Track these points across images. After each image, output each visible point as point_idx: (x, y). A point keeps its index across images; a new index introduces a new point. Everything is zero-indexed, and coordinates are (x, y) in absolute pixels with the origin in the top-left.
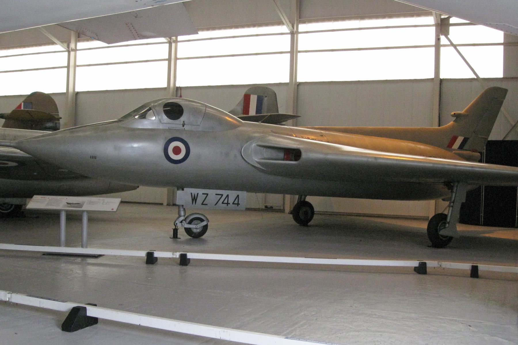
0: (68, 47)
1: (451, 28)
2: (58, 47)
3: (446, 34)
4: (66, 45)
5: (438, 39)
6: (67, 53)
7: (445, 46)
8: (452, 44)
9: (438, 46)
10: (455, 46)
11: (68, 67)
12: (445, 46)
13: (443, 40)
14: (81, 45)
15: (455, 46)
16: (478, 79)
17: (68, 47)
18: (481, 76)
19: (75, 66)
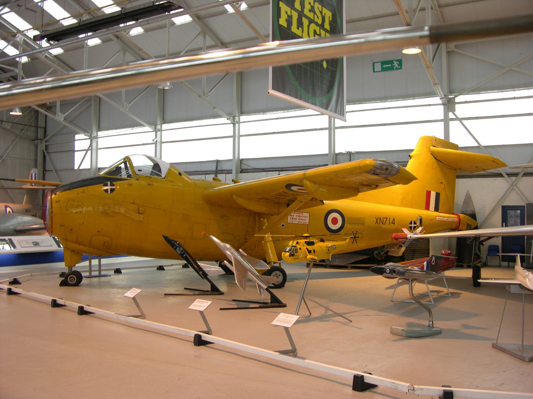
0: (155, 128)
1: (457, 106)
2: (147, 128)
3: (453, 111)
4: (153, 127)
6: (154, 133)
7: (452, 119)
8: (457, 119)
9: (446, 121)
10: (461, 120)
11: (156, 143)
12: (452, 119)
13: (451, 115)
14: (165, 126)
15: (461, 120)
17: (155, 128)
18: (483, 144)
19: (162, 143)
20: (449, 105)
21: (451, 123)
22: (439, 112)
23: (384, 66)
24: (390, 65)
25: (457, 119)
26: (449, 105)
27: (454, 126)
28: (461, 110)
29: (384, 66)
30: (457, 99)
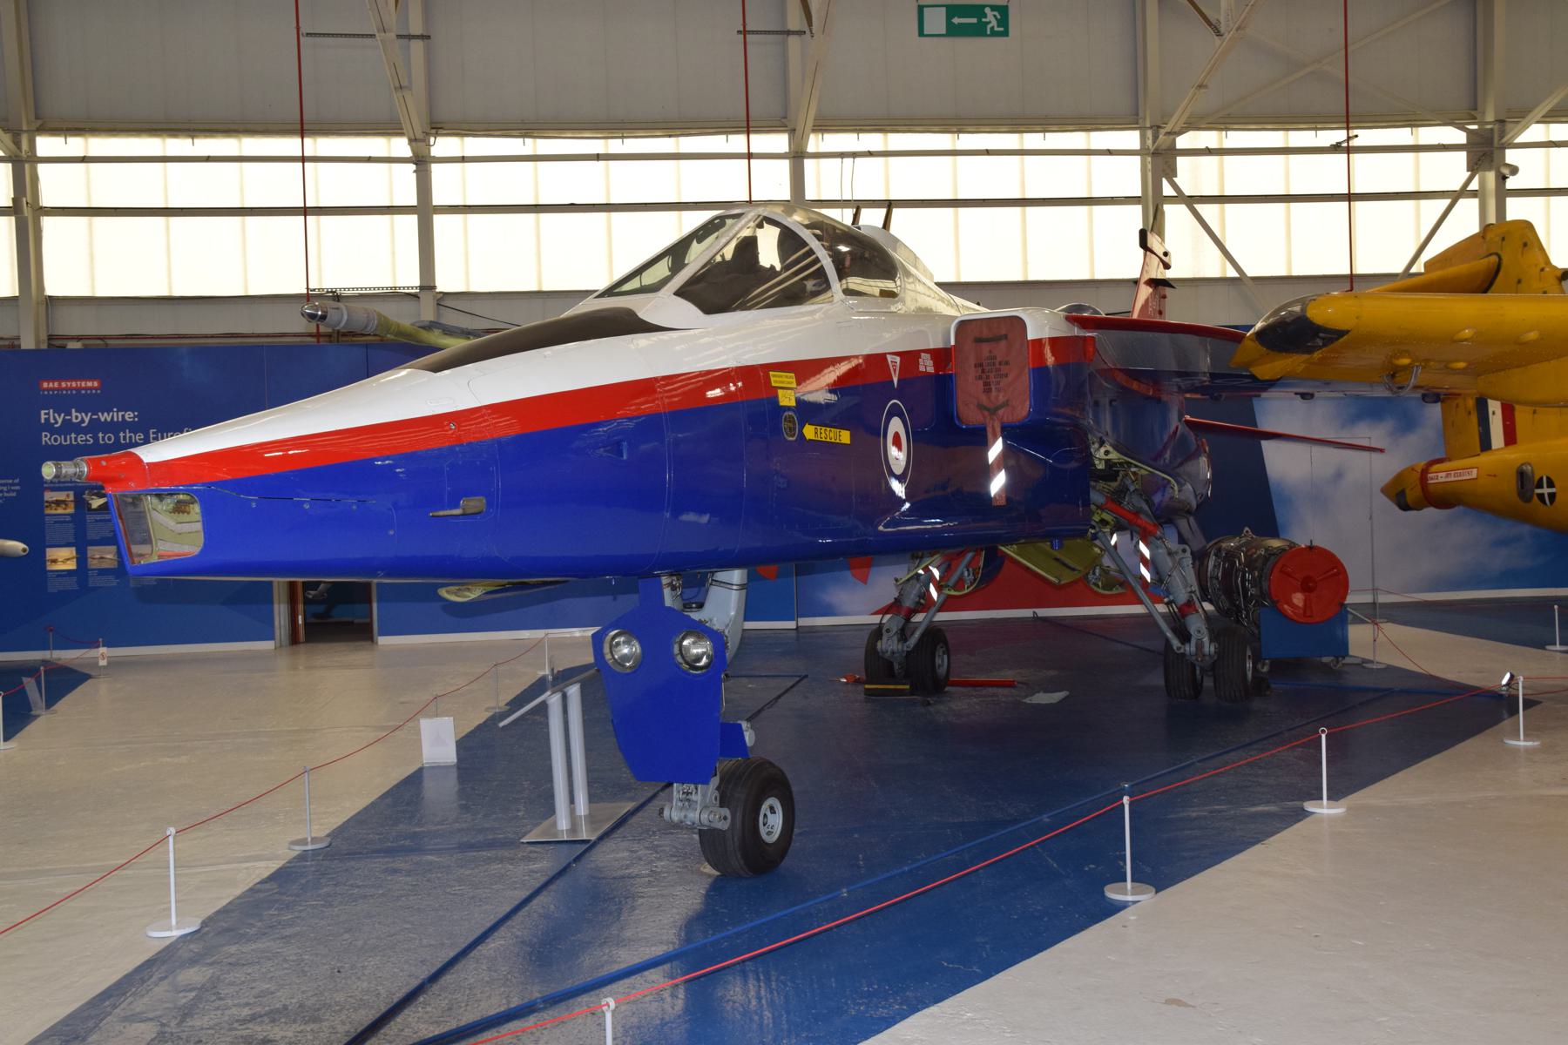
1: (1180, 160)
3: (1171, 173)
5: (1158, 188)
8: (1180, 198)
10: (1191, 201)
13: (1168, 190)
16: (1241, 283)
18: (1251, 272)
20: (1161, 160)
21: (1167, 208)
22: (1127, 176)
23: (956, 21)
24: (974, 20)
25: (1180, 198)
26: (1161, 160)
27: (1175, 214)
28: (1192, 175)
29: (956, 21)
30: (1183, 142)
